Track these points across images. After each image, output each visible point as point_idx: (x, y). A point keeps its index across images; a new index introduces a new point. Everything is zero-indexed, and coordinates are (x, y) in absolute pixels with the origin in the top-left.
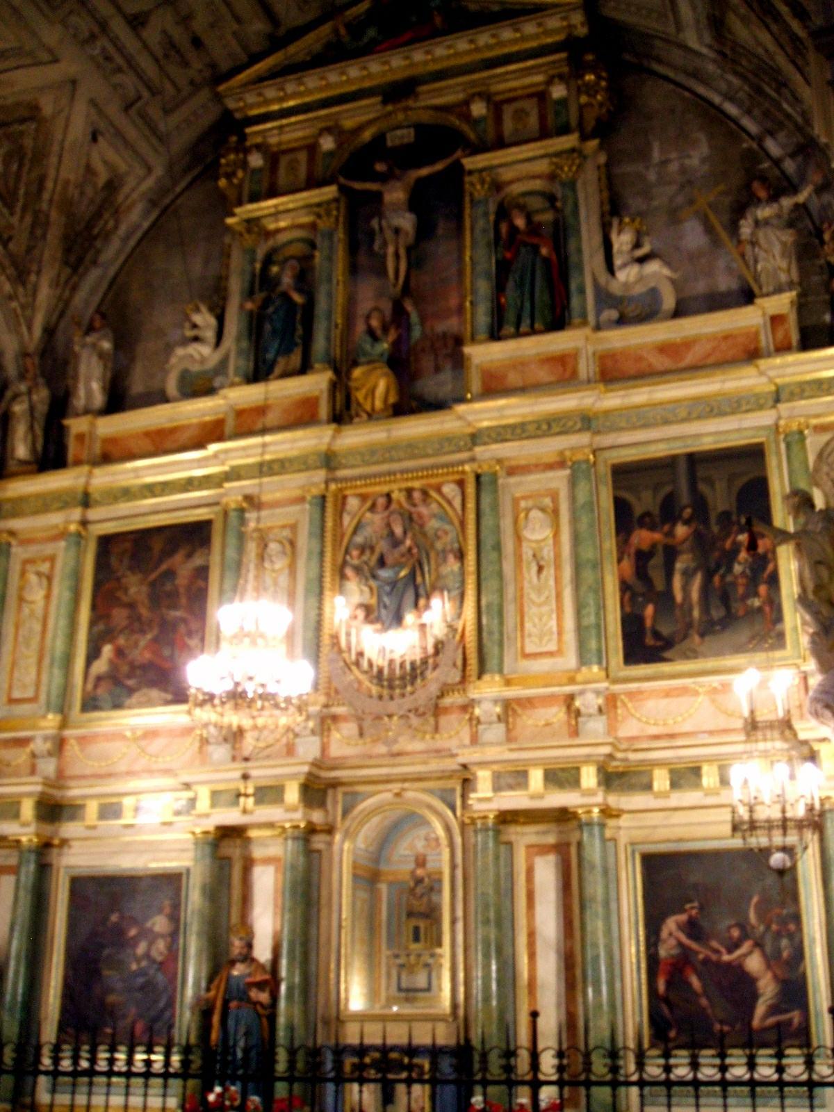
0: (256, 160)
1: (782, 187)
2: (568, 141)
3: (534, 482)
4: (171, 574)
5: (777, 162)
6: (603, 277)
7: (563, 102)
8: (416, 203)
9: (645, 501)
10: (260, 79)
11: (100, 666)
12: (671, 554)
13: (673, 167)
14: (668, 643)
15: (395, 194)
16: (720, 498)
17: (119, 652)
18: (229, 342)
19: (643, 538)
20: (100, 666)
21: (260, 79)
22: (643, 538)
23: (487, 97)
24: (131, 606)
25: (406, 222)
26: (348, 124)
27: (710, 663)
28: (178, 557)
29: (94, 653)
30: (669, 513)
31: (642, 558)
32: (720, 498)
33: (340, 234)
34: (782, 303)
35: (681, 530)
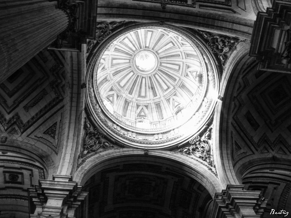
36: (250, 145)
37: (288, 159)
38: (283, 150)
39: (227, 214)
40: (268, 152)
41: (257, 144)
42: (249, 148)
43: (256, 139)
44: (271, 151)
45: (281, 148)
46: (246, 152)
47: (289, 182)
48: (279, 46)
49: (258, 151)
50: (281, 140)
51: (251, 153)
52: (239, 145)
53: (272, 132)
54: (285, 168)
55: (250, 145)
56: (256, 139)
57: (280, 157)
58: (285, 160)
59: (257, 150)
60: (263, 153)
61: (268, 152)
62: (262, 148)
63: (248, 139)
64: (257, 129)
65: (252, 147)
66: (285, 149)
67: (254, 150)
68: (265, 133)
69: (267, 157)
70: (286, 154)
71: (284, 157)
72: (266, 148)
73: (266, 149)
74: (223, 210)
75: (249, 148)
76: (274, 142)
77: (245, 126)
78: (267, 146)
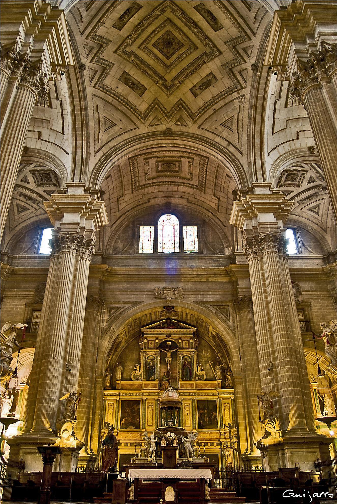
0: (146, 341)
1: (220, 363)
2: (193, 350)
3: (187, 401)
4: (134, 408)
5: (219, 358)
6: (197, 372)
7: (192, 342)
8: (171, 356)
9: (201, 406)
10: (148, 329)
11: (123, 422)
12: (204, 414)
13: (206, 355)
14: (204, 426)
15: (169, 355)
16: (211, 407)
17: (126, 420)
18: (141, 372)
19: (201, 411)
20: (123, 422)
21: (148, 329)
22: (201, 411)
23: (181, 339)
24: (128, 413)
25: (170, 359)
26: (160, 338)
27: (209, 430)
28: (135, 406)
29: (121, 420)
30: (204, 409)
31: (201, 414)
32: (211, 407)
33: (159, 357)
34: (220, 381)
35: (206, 411)
36: (93, 25)
37: (86, 86)
38: (94, 76)
39: (25, 24)
40: (87, 55)
41: (95, 35)
42: (89, 25)
43: (101, 31)
44: (90, 58)
45: (96, 71)
46: (82, 22)
47: (48, 99)
48: (328, 35)
49: (86, 40)
50: (108, 68)
51: (82, 29)
52: (93, 6)
53: (115, 52)
54: (73, 87)
55: (93, 25)
56: (101, 31)
57: (85, 75)
58: (83, 82)
59: (87, 38)
60: (84, 47)
61: (87, 55)
62: (91, 44)
63: (100, 19)
64: (116, 28)
65: (90, 29)
66: (96, 78)
67: (87, 32)
68: (111, 41)
69: (81, 56)
70: (91, 81)
71: (87, 80)
72: (92, 49)
73: (90, 52)
74: (29, 12)
75: (89, 25)
76: (103, 59)
77: (119, 7)
78: (95, 51)
